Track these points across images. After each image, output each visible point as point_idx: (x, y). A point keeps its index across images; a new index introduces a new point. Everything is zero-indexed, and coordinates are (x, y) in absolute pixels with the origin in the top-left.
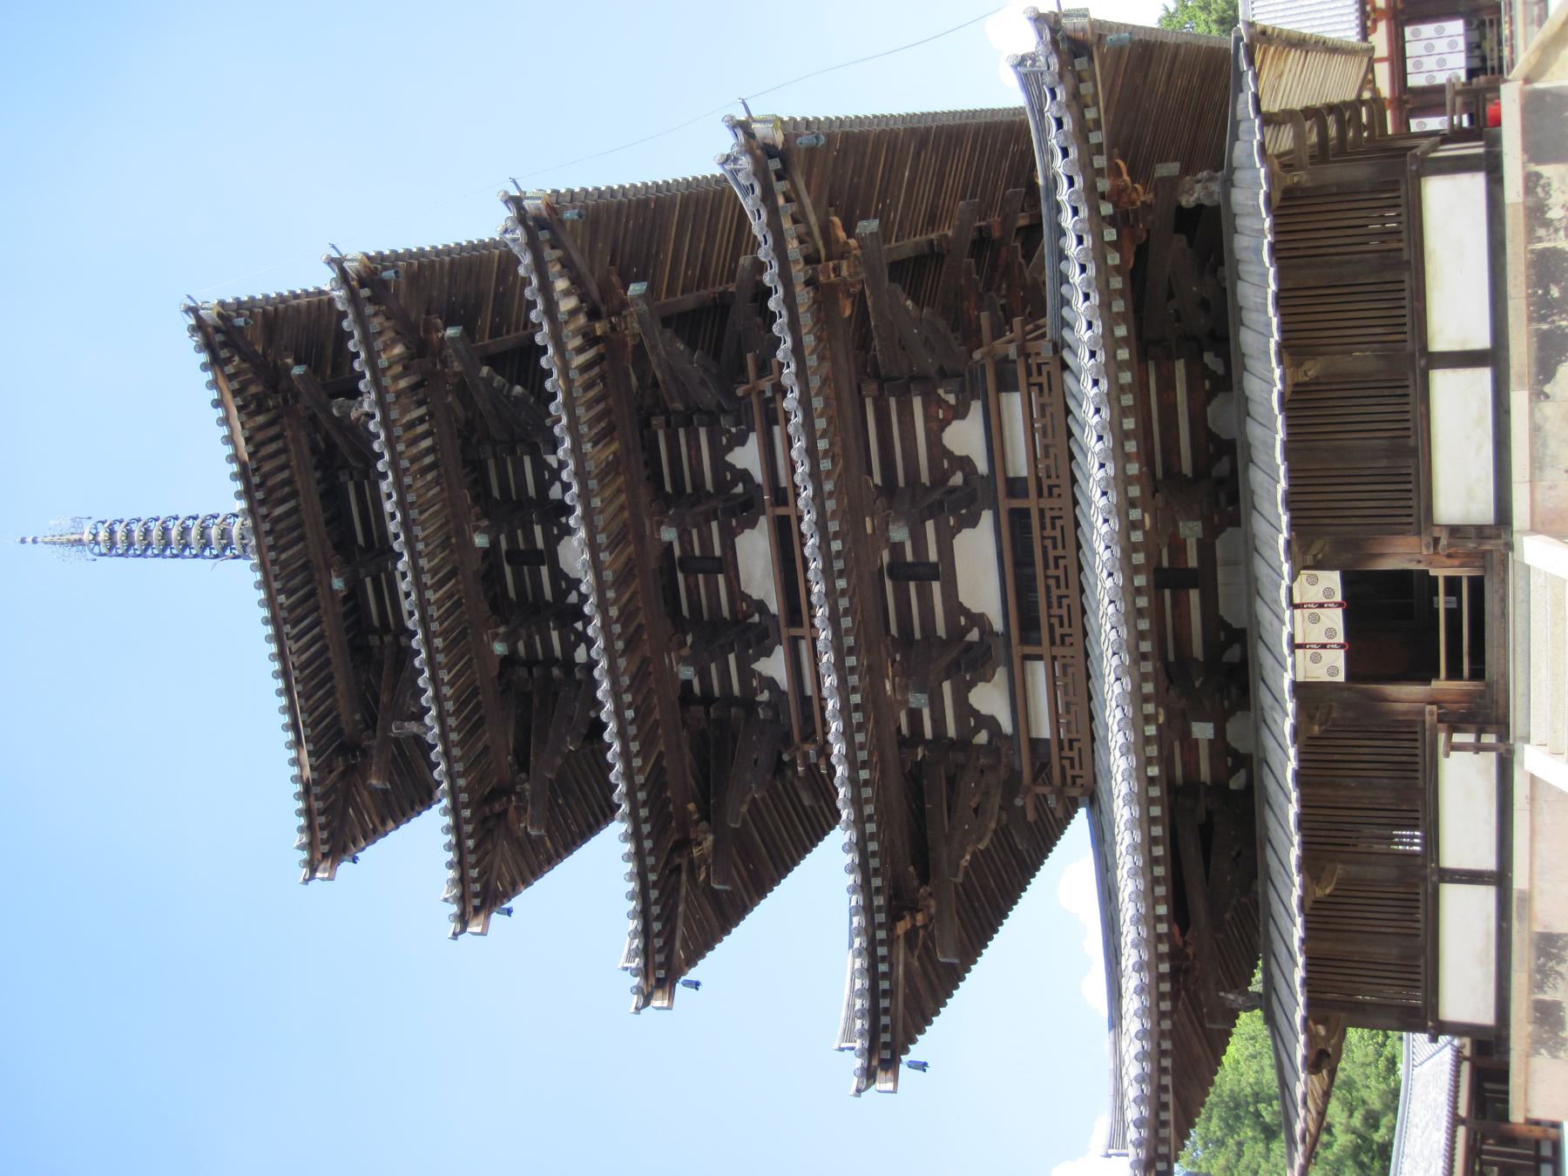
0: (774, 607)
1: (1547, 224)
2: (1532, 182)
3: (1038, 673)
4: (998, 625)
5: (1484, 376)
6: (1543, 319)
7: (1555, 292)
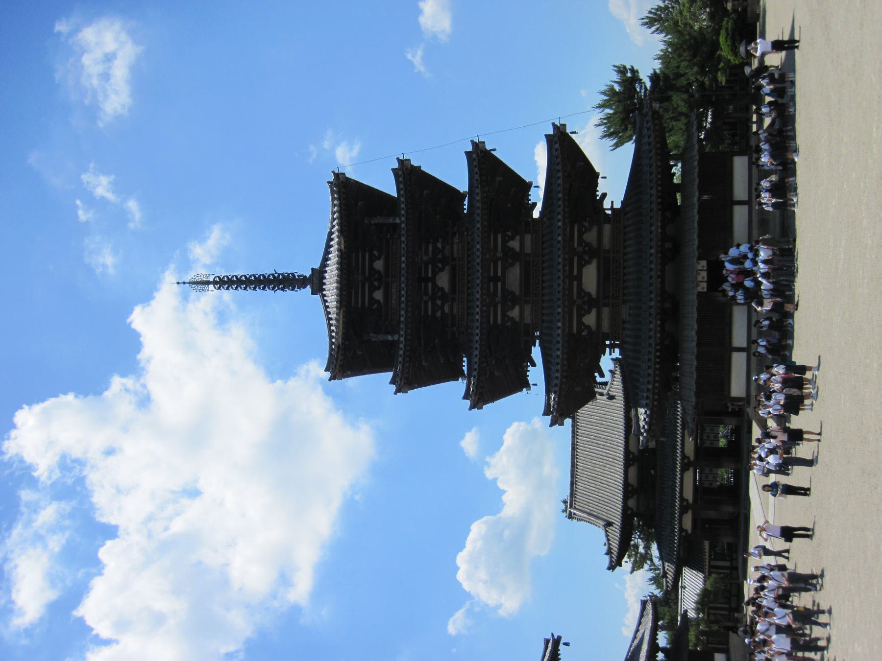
3: (606, 311)
5: (746, 207)
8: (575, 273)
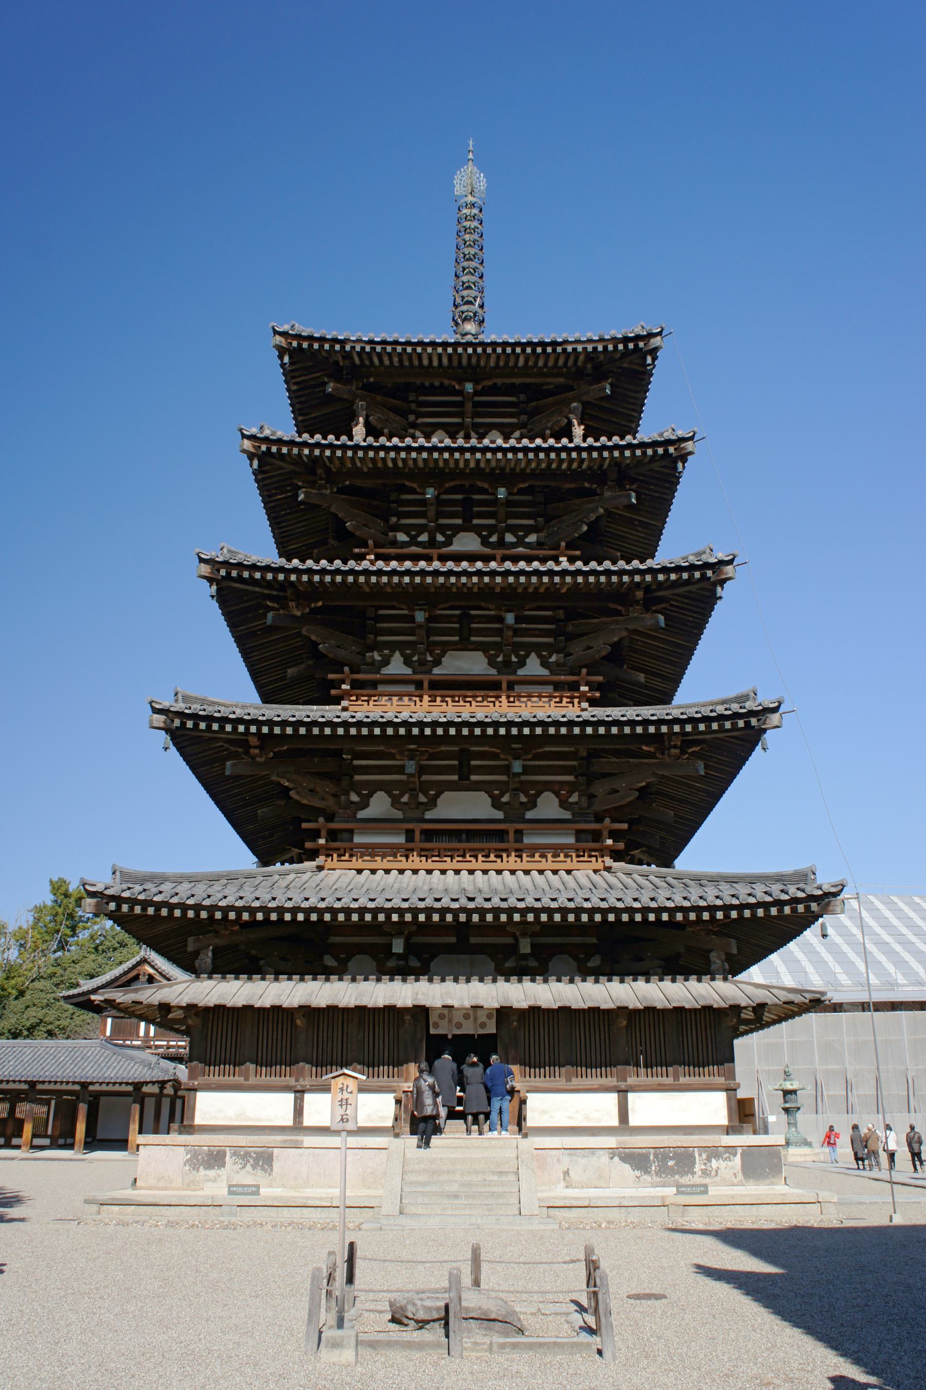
0: (436, 671)
1: (709, 1159)
2: (731, 1149)
4: (429, 815)
6: (656, 1156)
7: (671, 1163)
8: (474, 778)
